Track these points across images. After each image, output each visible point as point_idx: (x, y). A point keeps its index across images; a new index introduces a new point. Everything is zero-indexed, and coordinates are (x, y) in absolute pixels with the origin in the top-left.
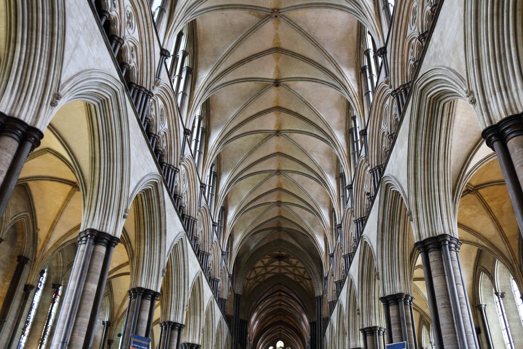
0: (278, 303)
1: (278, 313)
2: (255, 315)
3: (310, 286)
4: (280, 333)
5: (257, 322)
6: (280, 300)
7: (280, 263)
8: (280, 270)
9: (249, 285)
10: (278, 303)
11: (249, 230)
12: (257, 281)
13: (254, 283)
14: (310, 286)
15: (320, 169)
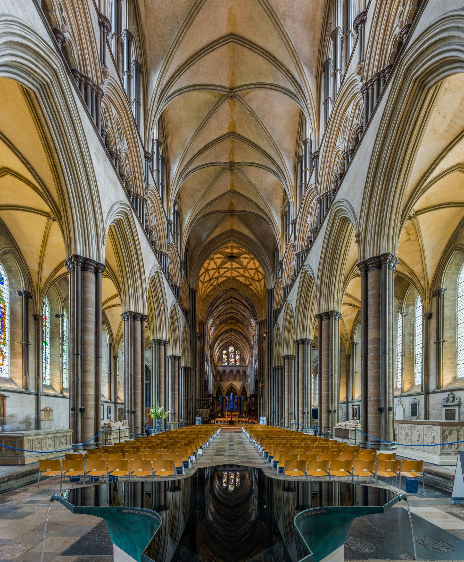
0: (230, 311)
1: (230, 321)
2: (211, 321)
3: (259, 288)
4: (231, 340)
5: (213, 328)
6: (232, 308)
7: (232, 265)
8: (232, 273)
9: (204, 289)
10: (230, 311)
11: (199, 207)
12: (211, 285)
13: (208, 286)
14: (259, 288)
15: (295, 54)
